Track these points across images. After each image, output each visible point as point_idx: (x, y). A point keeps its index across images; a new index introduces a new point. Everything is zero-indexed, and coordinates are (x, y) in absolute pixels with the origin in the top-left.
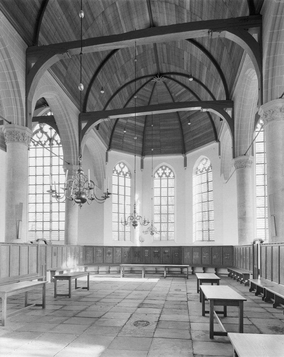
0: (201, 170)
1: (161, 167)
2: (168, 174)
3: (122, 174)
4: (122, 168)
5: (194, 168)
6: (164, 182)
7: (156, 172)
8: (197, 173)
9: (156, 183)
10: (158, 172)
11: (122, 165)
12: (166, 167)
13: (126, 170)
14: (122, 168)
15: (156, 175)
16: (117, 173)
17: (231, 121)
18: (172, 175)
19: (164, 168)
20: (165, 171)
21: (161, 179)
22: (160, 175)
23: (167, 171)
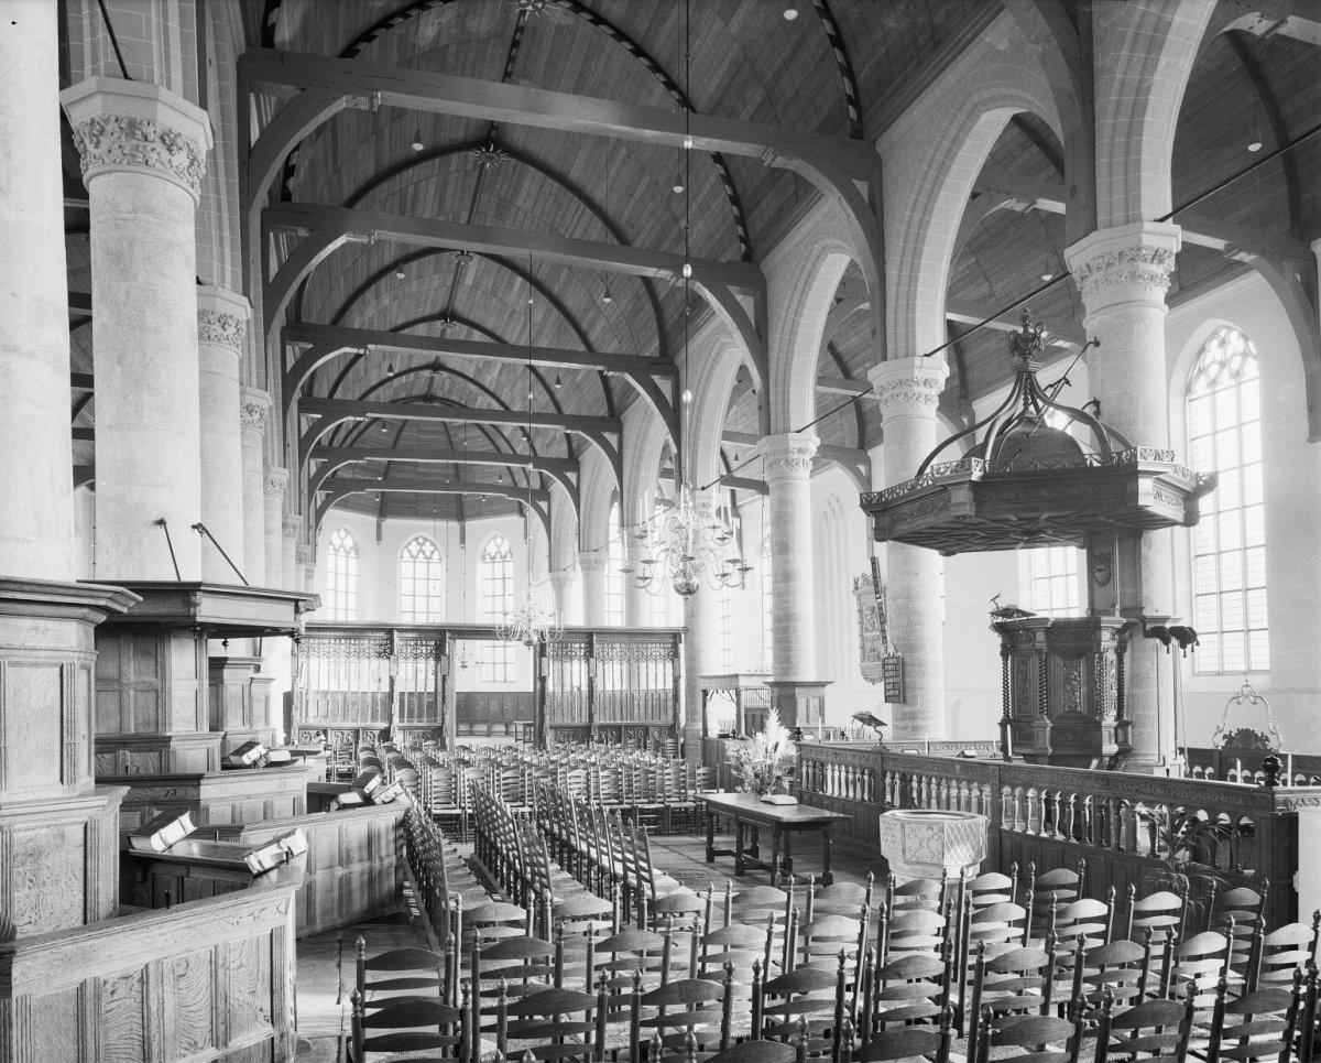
0: (493, 554)
1: (416, 539)
2: (428, 554)
3: (342, 550)
4: (342, 540)
5: (481, 546)
6: (421, 568)
7: (406, 547)
8: (484, 558)
9: (406, 568)
10: (410, 547)
11: (342, 533)
12: (426, 539)
13: (349, 543)
14: (342, 540)
15: (405, 553)
16: (335, 549)
17: (575, 493)
18: (436, 556)
19: (421, 541)
20: (424, 548)
21: (415, 563)
22: (414, 554)
23: (428, 548)
